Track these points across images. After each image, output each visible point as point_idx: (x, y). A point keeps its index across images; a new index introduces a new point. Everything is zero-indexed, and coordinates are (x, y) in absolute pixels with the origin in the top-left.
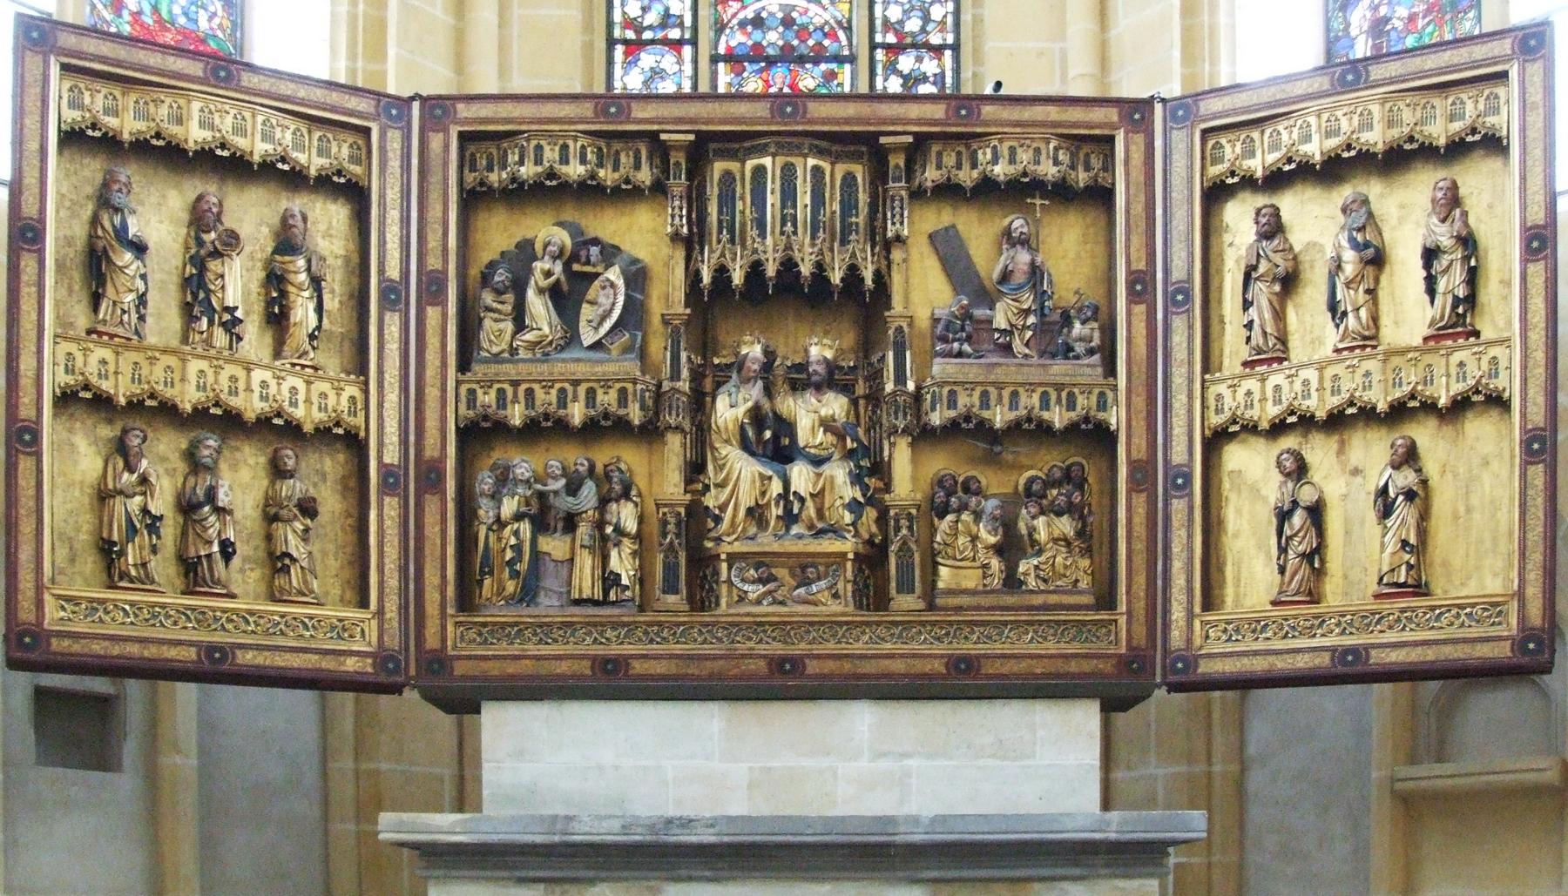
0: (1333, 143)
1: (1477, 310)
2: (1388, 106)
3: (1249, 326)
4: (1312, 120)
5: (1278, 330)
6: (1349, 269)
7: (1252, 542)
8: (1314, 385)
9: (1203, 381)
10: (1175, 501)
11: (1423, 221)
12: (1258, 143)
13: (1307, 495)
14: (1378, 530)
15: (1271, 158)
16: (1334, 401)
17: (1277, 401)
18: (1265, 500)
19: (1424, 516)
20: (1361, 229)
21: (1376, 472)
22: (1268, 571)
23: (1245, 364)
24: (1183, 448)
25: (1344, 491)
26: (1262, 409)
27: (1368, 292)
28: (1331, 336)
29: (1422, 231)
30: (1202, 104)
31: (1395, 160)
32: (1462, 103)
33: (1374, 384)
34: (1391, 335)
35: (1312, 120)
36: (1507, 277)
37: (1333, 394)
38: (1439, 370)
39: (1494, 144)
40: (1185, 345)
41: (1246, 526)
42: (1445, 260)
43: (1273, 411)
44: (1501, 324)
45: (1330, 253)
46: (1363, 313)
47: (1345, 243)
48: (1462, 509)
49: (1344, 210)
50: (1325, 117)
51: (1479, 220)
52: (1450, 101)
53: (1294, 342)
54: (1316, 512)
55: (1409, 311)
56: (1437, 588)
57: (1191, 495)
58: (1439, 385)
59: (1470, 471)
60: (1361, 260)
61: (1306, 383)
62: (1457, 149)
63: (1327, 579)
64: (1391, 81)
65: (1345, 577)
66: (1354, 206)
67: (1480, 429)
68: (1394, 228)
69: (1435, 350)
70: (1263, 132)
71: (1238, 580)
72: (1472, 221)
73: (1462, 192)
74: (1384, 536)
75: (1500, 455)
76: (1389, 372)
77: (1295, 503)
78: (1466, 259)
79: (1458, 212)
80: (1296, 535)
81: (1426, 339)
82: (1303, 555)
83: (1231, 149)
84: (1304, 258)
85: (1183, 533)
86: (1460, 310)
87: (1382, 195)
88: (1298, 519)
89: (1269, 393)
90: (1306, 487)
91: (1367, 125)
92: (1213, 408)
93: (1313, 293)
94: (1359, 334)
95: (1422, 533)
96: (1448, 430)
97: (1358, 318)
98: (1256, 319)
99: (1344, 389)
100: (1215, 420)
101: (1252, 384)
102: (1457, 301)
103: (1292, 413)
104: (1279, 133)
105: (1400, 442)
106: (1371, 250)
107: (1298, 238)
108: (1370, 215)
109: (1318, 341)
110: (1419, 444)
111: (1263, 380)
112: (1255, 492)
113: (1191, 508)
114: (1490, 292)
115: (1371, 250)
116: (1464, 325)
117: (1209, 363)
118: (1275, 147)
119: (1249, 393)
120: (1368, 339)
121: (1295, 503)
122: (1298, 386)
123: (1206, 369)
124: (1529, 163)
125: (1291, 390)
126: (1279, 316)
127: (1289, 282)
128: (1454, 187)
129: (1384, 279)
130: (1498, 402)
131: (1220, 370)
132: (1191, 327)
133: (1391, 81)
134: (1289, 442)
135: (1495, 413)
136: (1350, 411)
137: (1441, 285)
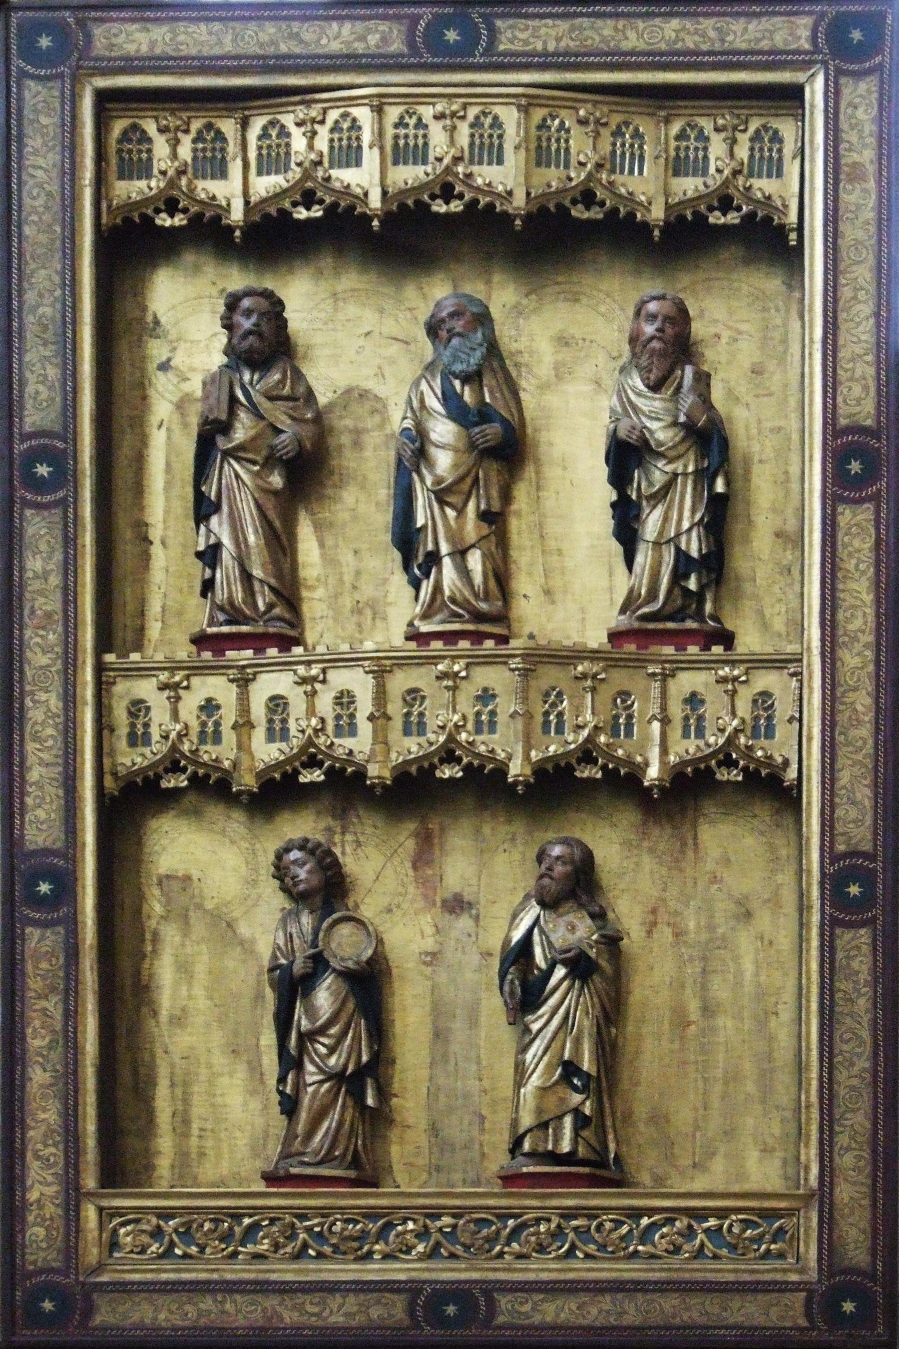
0: (408, 175)
1: (724, 590)
2: (538, 114)
3: (210, 555)
4: (363, 115)
5: (279, 576)
6: (444, 462)
7: (217, 1038)
8: (365, 706)
9: (100, 668)
10: (33, 934)
11: (610, 381)
12: (232, 148)
13: (346, 945)
14: (507, 1036)
15: (265, 185)
16: (412, 747)
17: (277, 731)
18: (247, 947)
19: (611, 1014)
20: (472, 378)
21: (503, 911)
22: (255, 1105)
23: (200, 641)
24: (52, 812)
25: (429, 944)
26: (242, 746)
27: (485, 516)
28: (401, 606)
29: (608, 402)
30: (98, 31)
31: (556, 238)
32: (702, 137)
33: (502, 718)
34: (538, 616)
35: (363, 115)
36: (791, 525)
37: (407, 732)
38: (645, 706)
39: (769, 241)
40: (55, 580)
41: (202, 1003)
42: (659, 473)
43: (266, 752)
44: (778, 624)
45: (398, 418)
46: (475, 561)
47: (434, 403)
48: (693, 1007)
49: (433, 329)
50: (393, 113)
51: (732, 396)
52: (675, 128)
53: (315, 605)
54: (369, 985)
55: (578, 576)
56: (644, 1166)
57: (72, 924)
58: (646, 738)
59: (711, 928)
60: (472, 445)
61: (345, 699)
62: (685, 239)
63: (394, 1134)
64: (545, 61)
65: (434, 1130)
66: (458, 325)
67: (731, 842)
68: (544, 387)
69: (639, 663)
70: (245, 124)
71: (182, 1120)
72: (717, 396)
73: (698, 329)
74: (524, 1049)
75: (774, 901)
76: (535, 697)
77: (319, 963)
78: (705, 477)
79: (689, 370)
80: (322, 1031)
81: (615, 636)
82: (338, 1077)
83: (168, 150)
84: (343, 423)
85: (53, 1005)
86: (692, 584)
87: (518, 311)
88: (324, 998)
89: (258, 711)
90: (345, 930)
91: (489, 149)
92: (123, 731)
93: (362, 502)
94: (465, 604)
95: (608, 1050)
96: (662, 837)
97: (464, 572)
98: (226, 541)
99: (432, 723)
100: (131, 759)
101: (218, 687)
102: (684, 564)
103: (313, 762)
104: (284, 133)
105: (557, 851)
106: (493, 430)
107: (325, 377)
108: (493, 349)
109: (374, 610)
110: (599, 855)
111: (244, 682)
112: (224, 928)
113: (73, 953)
114: (756, 552)
115: (493, 430)
116: (699, 615)
117: (116, 627)
118: (273, 160)
119: (209, 707)
120: (487, 619)
121: (319, 963)
122: (325, 704)
123: (105, 641)
124: (846, 293)
125: (311, 711)
126: (281, 543)
127: (304, 471)
128: (680, 318)
129: (522, 493)
130: (772, 790)
131: (138, 646)
132: (70, 542)
133: (545, 61)
134: (301, 825)
135: (763, 811)
136: (446, 772)
137: (652, 523)
